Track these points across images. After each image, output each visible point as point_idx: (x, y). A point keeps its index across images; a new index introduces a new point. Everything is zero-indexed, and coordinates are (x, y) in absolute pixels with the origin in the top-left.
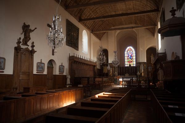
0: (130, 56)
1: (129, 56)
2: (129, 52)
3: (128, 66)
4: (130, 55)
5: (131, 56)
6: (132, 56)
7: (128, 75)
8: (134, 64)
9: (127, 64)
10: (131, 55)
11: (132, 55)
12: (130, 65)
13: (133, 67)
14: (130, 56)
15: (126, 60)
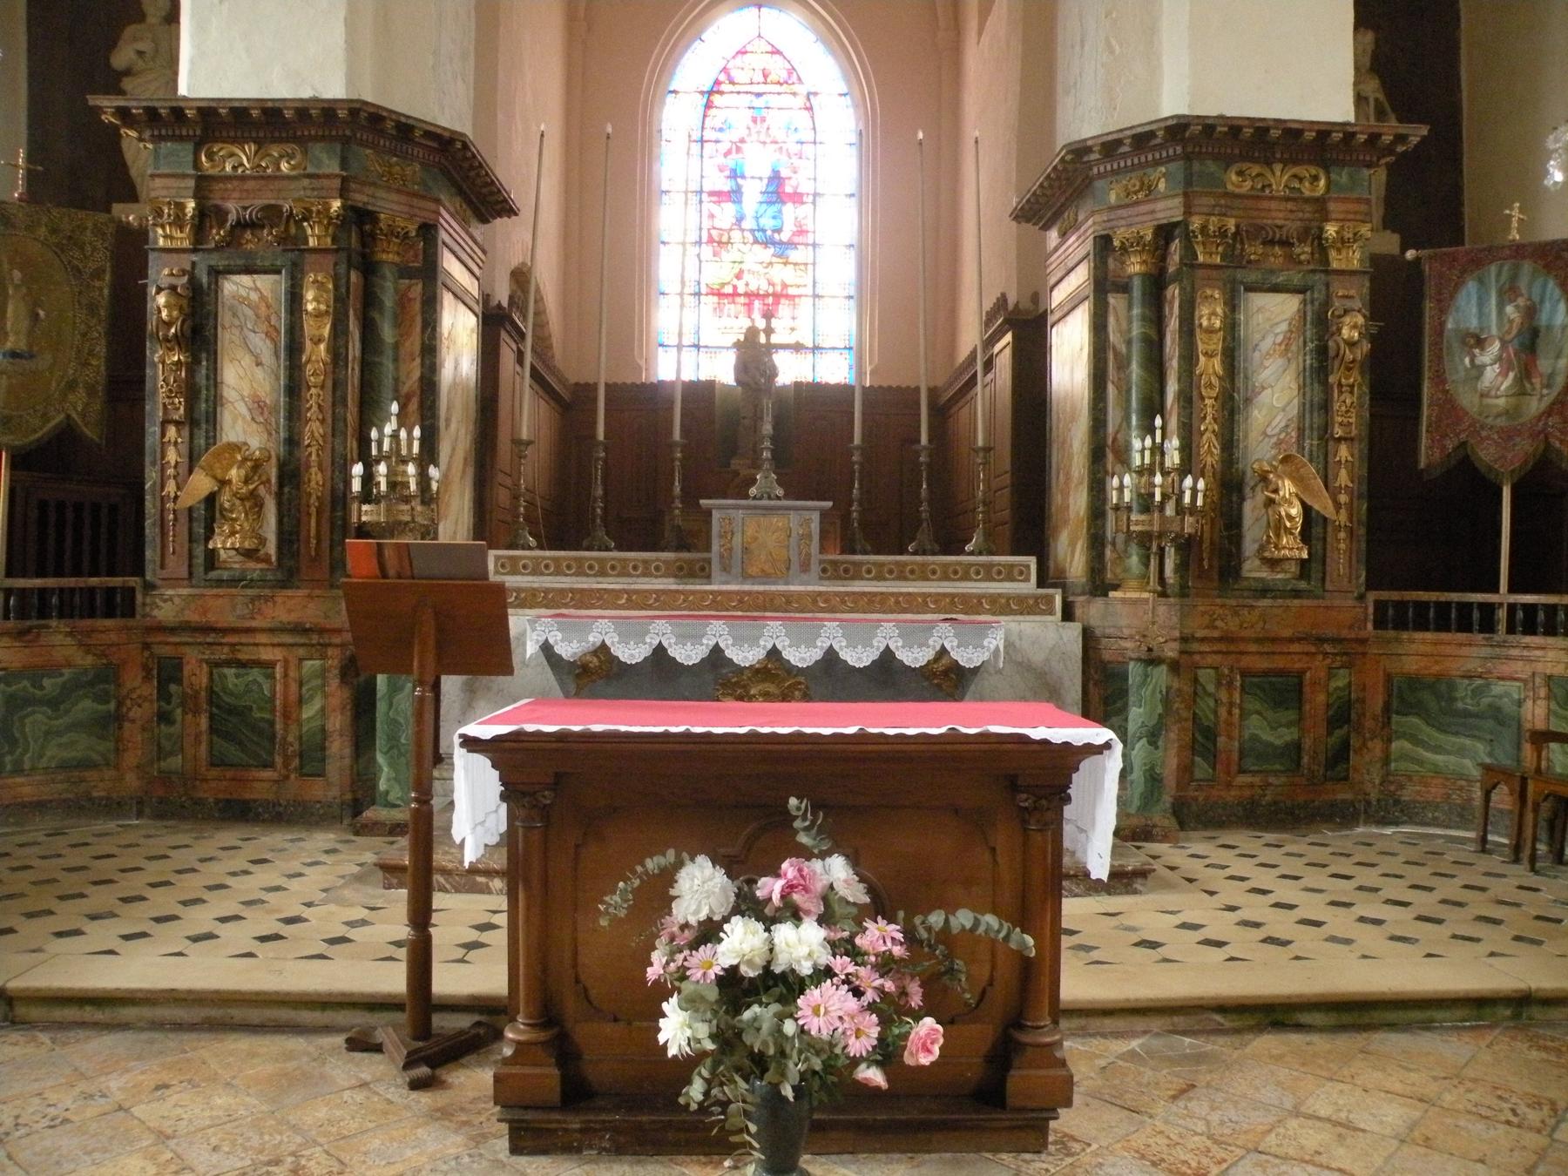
0: (753, 192)
1: (734, 195)
2: (733, 111)
3: (722, 370)
4: (758, 163)
5: (778, 191)
6: (797, 198)
7: (807, 517)
8: (824, 346)
9: (689, 346)
10: (776, 179)
11: (799, 181)
12: (754, 356)
13: (812, 396)
14: (753, 192)
15: (671, 266)
